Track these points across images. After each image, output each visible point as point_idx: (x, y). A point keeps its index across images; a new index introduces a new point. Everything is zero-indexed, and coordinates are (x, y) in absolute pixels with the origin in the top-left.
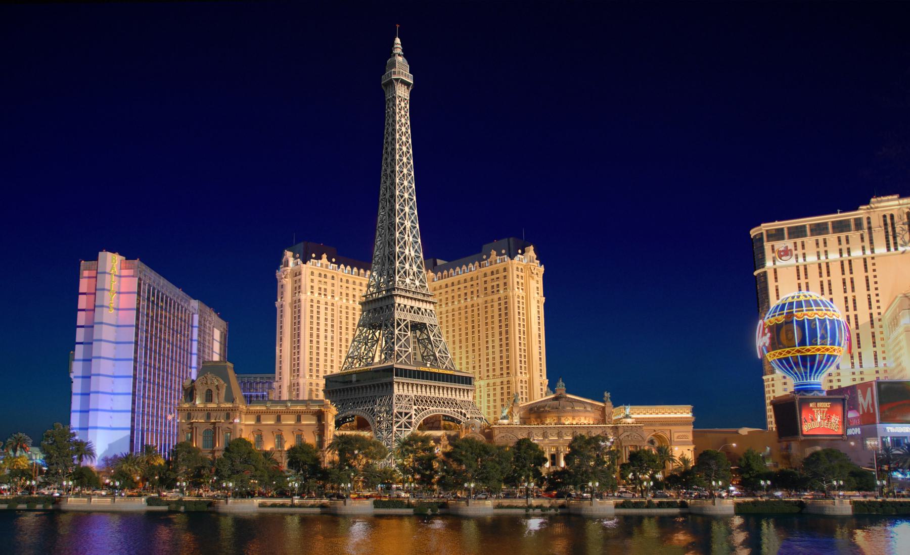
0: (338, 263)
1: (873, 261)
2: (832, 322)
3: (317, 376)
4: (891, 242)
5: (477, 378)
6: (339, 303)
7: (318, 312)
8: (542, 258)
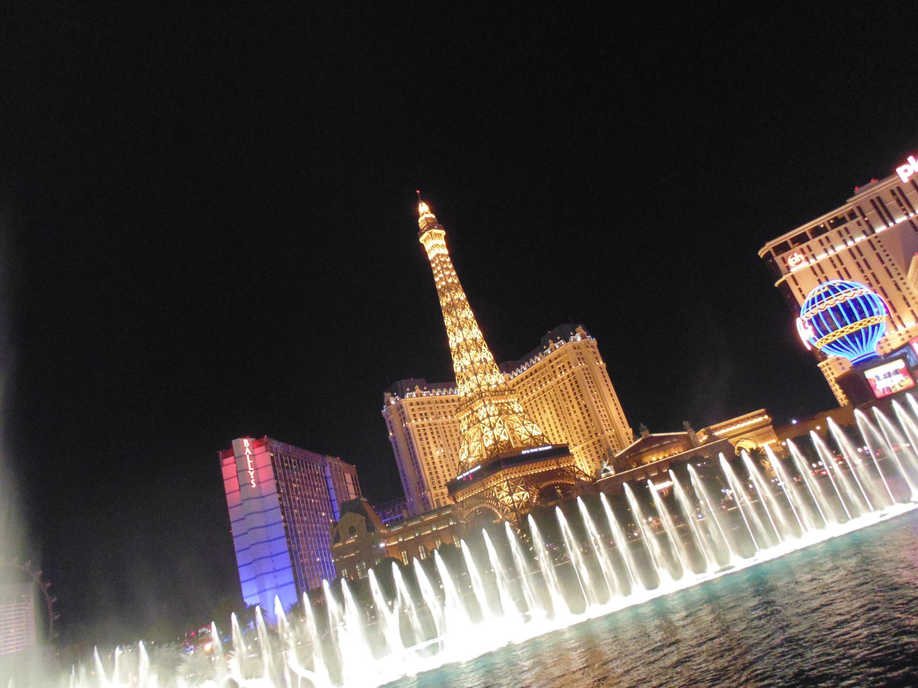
0: (429, 389)
4: (887, 218)
5: (571, 444)
7: (425, 434)
8: (591, 331)
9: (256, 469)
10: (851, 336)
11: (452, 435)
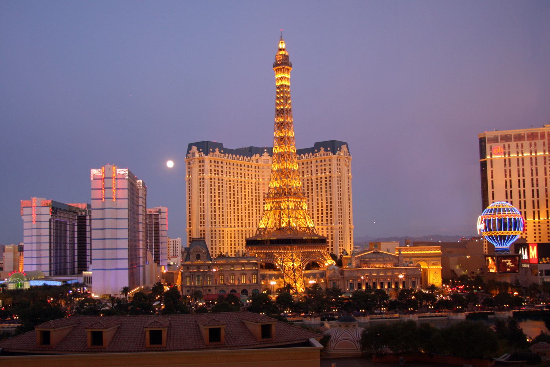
2: (515, 219)
3: (215, 226)
6: (226, 179)
10: (500, 236)
11: (245, 203)
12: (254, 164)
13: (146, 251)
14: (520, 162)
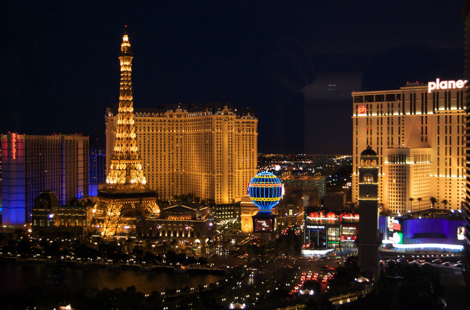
1: (403, 119)
4: (413, 109)
9: (17, 150)
10: (257, 202)
12: (168, 118)
13: (87, 185)
14: (380, 121)
